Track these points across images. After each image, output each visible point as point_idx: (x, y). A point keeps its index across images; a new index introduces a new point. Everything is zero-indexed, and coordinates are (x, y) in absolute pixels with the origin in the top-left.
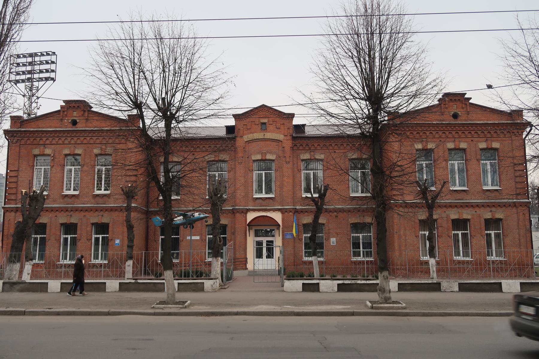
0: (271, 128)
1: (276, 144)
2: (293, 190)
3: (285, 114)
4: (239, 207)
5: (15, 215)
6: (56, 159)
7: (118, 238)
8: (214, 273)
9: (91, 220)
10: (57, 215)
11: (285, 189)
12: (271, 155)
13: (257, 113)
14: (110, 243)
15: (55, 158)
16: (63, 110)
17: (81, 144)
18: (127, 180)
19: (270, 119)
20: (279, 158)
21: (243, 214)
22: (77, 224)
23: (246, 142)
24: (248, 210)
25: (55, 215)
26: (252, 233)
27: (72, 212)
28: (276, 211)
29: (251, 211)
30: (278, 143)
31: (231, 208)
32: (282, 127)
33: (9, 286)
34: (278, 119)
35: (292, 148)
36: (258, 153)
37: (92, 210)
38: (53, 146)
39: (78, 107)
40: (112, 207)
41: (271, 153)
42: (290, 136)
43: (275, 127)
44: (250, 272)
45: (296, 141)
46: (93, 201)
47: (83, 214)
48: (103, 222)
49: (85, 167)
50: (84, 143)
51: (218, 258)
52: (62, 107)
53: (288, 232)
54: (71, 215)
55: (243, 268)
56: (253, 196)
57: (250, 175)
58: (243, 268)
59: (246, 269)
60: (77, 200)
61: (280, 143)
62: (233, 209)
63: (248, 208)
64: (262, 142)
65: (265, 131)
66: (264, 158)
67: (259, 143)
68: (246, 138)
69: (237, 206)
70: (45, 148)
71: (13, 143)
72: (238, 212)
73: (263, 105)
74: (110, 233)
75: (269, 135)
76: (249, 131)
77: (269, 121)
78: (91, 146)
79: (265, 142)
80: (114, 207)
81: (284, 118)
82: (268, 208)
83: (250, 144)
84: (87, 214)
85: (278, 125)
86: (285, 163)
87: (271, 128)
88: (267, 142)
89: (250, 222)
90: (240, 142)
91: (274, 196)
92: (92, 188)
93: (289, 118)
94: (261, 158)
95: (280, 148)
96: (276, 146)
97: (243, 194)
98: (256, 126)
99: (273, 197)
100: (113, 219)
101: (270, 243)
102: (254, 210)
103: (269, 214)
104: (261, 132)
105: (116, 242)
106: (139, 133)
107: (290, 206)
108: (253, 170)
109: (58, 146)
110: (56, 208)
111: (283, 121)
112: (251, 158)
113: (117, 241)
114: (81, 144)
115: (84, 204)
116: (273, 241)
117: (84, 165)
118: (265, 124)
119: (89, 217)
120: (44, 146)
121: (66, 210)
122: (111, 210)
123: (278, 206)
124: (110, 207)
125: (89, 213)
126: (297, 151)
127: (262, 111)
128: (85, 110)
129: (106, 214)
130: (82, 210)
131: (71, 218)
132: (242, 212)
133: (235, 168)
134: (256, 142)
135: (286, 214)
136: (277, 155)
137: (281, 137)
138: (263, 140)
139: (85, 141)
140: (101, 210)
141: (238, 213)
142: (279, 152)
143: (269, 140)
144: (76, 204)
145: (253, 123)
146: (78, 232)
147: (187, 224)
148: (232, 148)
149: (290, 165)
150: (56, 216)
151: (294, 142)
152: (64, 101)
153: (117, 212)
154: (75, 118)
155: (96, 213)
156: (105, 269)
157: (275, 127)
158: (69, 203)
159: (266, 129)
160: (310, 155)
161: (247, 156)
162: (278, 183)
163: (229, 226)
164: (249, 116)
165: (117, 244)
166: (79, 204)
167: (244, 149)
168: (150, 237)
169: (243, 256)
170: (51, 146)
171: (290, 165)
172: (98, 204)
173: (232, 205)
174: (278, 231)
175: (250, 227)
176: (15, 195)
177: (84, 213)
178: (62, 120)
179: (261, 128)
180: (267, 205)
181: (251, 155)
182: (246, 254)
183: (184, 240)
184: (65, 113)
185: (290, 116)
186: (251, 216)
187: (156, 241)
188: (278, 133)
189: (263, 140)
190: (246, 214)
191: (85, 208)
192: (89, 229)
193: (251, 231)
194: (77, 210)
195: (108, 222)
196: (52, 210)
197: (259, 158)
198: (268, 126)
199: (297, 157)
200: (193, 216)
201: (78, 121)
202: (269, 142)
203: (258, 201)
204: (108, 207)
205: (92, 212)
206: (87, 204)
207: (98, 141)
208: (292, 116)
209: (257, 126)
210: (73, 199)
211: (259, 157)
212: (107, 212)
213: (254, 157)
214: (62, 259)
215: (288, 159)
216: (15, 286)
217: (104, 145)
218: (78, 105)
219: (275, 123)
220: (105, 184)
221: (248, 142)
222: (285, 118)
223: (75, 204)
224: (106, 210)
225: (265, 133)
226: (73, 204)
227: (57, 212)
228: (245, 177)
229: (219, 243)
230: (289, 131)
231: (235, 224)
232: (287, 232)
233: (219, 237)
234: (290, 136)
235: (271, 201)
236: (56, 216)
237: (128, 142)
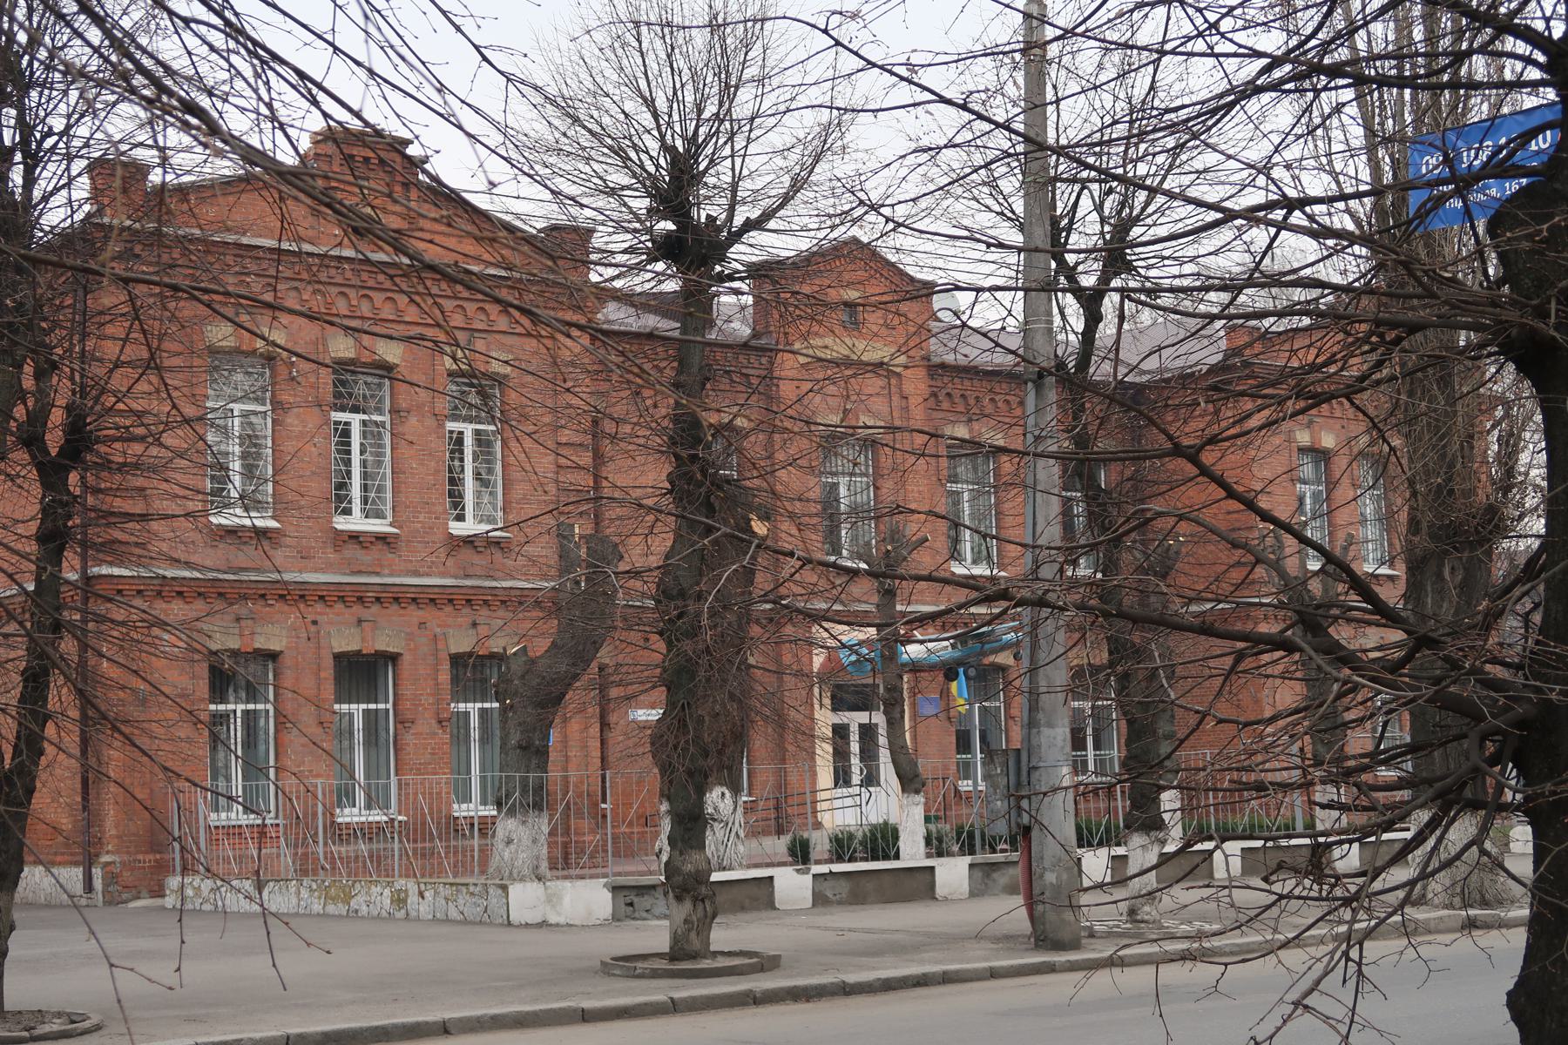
0: (874, 319)
9: (451, 641)
10: (319, 618)
33: (980, 874)
47: (414, 614)
50: (407, 319)
60: (390, 556)
87: (874, 319)
101: (867, 732)
115: (416, 574)
119: (438, 630)
121: (354, 597)
144: (391, 575)
151: (933, 383)
158: (363, 568)
160: (971, 431)
166: (399, 576)
177: (421, 613)
191: (429, 590)
194: (397, 598)
206: (428, 575)
216: (995, 875)
226: (377, 574)
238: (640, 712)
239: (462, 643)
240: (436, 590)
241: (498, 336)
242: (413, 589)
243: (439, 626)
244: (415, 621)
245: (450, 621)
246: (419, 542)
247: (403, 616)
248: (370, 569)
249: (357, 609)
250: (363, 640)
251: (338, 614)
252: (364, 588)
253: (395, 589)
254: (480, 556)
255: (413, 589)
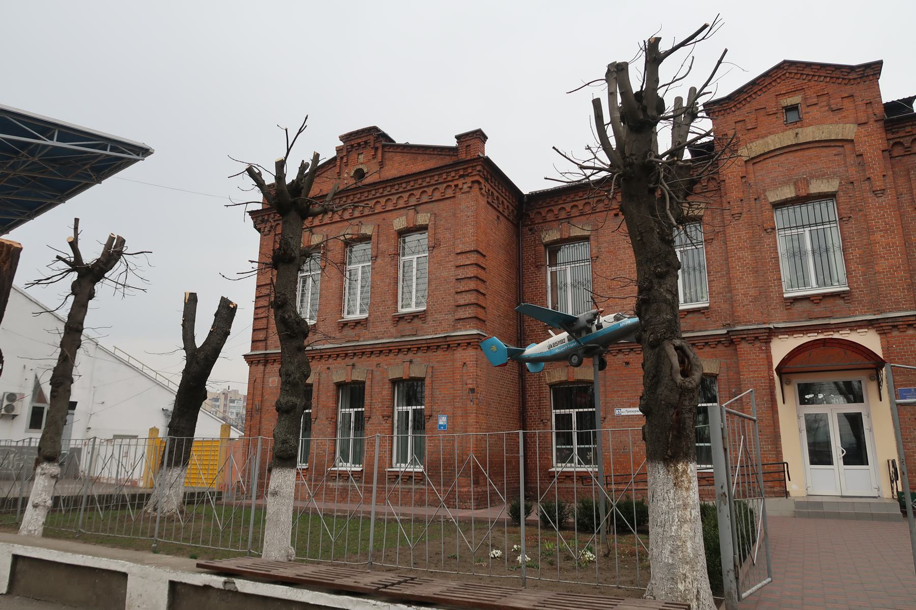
1: (834, 152)
2: (909, 266)
3: (851, 69)
4: (746, 325)
5: (264, 370)
6: (329, 253)
7: (444, 413)
8: (666, 553)
9: (390, 372)
10: (331, 366)
11: (882, 265)
12: (825, 181)
13: (769, 87)
14: (428, 425)
15: (329, 251)
16: (342, 155)
17: (371, 215)
18: (459, 277)
19: (810, 93)
20: (851, 186)
21: (758, 344)
22: (363, 383)
23: (746, 162)
24: (772, 333)
25: (328, 366)
26: (792, 392)
27: (355, 358)
28: (861, 327)
29: (783, 333)
30: (841, 149)
31: (724, 332)
32: (847, 104)
34: (831, 89)
35: (888, 153)
36: (785, 183)
37: (390, 351)
38: (325, 229)
39: (366, 143)
40: (428, 341)
41: (822, 176)
42: (876, 121)
43: (827, 108)
44: (798, 504)
45: (897, 132)
46: (393, 330)
47: (375, 359)
48: (413, 375)
49: (379, 260)
51: (680, 466)
52: (339, 150)
53: (911, 385)
54: (353, 365)
55: (776, 490)
56: (783, 293)
57: (767, 240)
58: (774, 492)
59: (787, 494)
61: (848, 146)
62: (728, 332)
63: (771, 326)
64: (791, 154)
65: (799, 124)
66: (803, 193)
67: (782, 158)
68: (744, 153)
69: (739, 323)
70: (313, 234)
71: (265, 233)
72: (744, 338)
73: (785, 62)
74: (427, 400)
75: (809, 134)
76: (752, 135)
77: (805, 99)
78: (389, 215)
79: (799, 153)
80: (432, 341)
81: (850, 80)
82: (833, 321)
83: (757, 166)
84: (382, 359)
85: (835, 102)
86: (870, 194)
88: (807, 153)
89: (784, 361)
90: (730, 170)
91: (848, 289)
92: (390, 302)
93: (868, 76)
94: (793, 195)
95: (851, 159)
96: (837, 158)
97: (752, 292)
98: (770, 118)
99: (844, 292)
100: (432, 367)
102: (790, 331)
103: (836, 336)
104: (786, 130)
105: (441, 423)
106: (479, 168)
107: (907, 310)
108: (774, 229)
109: (333, 226)
110: (328, 351)
111: (848, 90)
112: (766, 198)
113: (443, 420)
114: (371, 215)
115: (377, 338)
116: (861, 413)
117: (376, 257)
118: (794, 108)
120: (311, 231)
122: (429, 347)
123: (865, 314)
124: (424, 342)
125: (387, 358)
126: (906, 158)
127: (783, 77)
128: (377, 145)
129: (418, 358)
130: (372, 352)
131: (353, 370)
132: (757, 338)
133: (724, 232)
134: (775, 159)
135: (895, 333)
136: (842, 179)
137: (848, 130)
138: (796, 148)
139: (378, 209)
140: (409, 349)
141: (743, 342)
142: (847, 171)
143: (811, 146)
144: (364, 341)
145: (762, 112)
146: (367, 400)
147: (580, 352)
148: (712, 185)
149: (887, 199)
150: (328, 368)
151: (890, 136)
152: (342, 138)
153: (440, 353)
154: (361, 167)
155: (400, 355)
156: (248, 502)
157: (827, 108)
159: (801, 120)
161: (753, 197)
162: (857, 253)
163: (723, 377)
164: (748, 99)
165: (442, 425)
166: (368, 341)
167: (744, 180)
168: (530, 412)
169: (771, 458)
170: (322, 228)
171: (887, 199)
172: (402, 336)
173: (724, 323)
174: (873, 386)
175: (784, 376)
176: (264, 332)
177: (377, 359)
178: (339, 174)
179: (786, 121)
180: (829, 314)
181: (765, 191)
182: (779, 453)
183: (609, 416)
184: (345, 160)
185: (869, 72)
186: (781, 348)
187: (544, 422)
188: (837, 123)
189: (796, 148)
190: (768, 342)
192: (386, 392)
193: (786, 388)
195: (422, 376)
196: (322, 355)
197: (789, 196)
198: (804, 111)
199: (909, 175)
200: (599, 327)
201: (365, 170)
202: (812, 153)
203: (798, 306)
204: (420, 342)
205: (391, 355)
206: (382, 338)
207: (401, 203)
208: (875, 68)
209: (773, 119)
210: (358, 330)
211: (788, 193)
212: (419, 354)
213: (773, 197)
214: (397, 462)
215: (878, 184)
217: (413, 207)
218: (364, 139)
219: (825, 98)
220: (417, 291)
221: (754, 160)
222: (854, 79)
223: (362, 339)
224: (419, 348)
225: (799, 130)
226: (358, 341)
227: (331, 360)
228: (752, 248)
229: (679, 378)
230: (870, 110)
231: (738, 373)
232: (905, 385)
233: (677, 348)
234: (876, 121)
235: (840, 302)
236: (328, 368)
237: (459, 195)
238: (623, 410)
239: (396, 373)
240: (380, 346)
241: (424, 206)
242: (368, 347)
243: (386, 365)
244: (375, 363)
245: (392, 361)
246: (379, 322)
247: (369, 361)
248: (354, 339)
249: (349, 361)
250: (347, 375)
251: (339, 363)
252: (346, 349)
253: (361, 348)
254: (410, 325)
255: (368, 347)
